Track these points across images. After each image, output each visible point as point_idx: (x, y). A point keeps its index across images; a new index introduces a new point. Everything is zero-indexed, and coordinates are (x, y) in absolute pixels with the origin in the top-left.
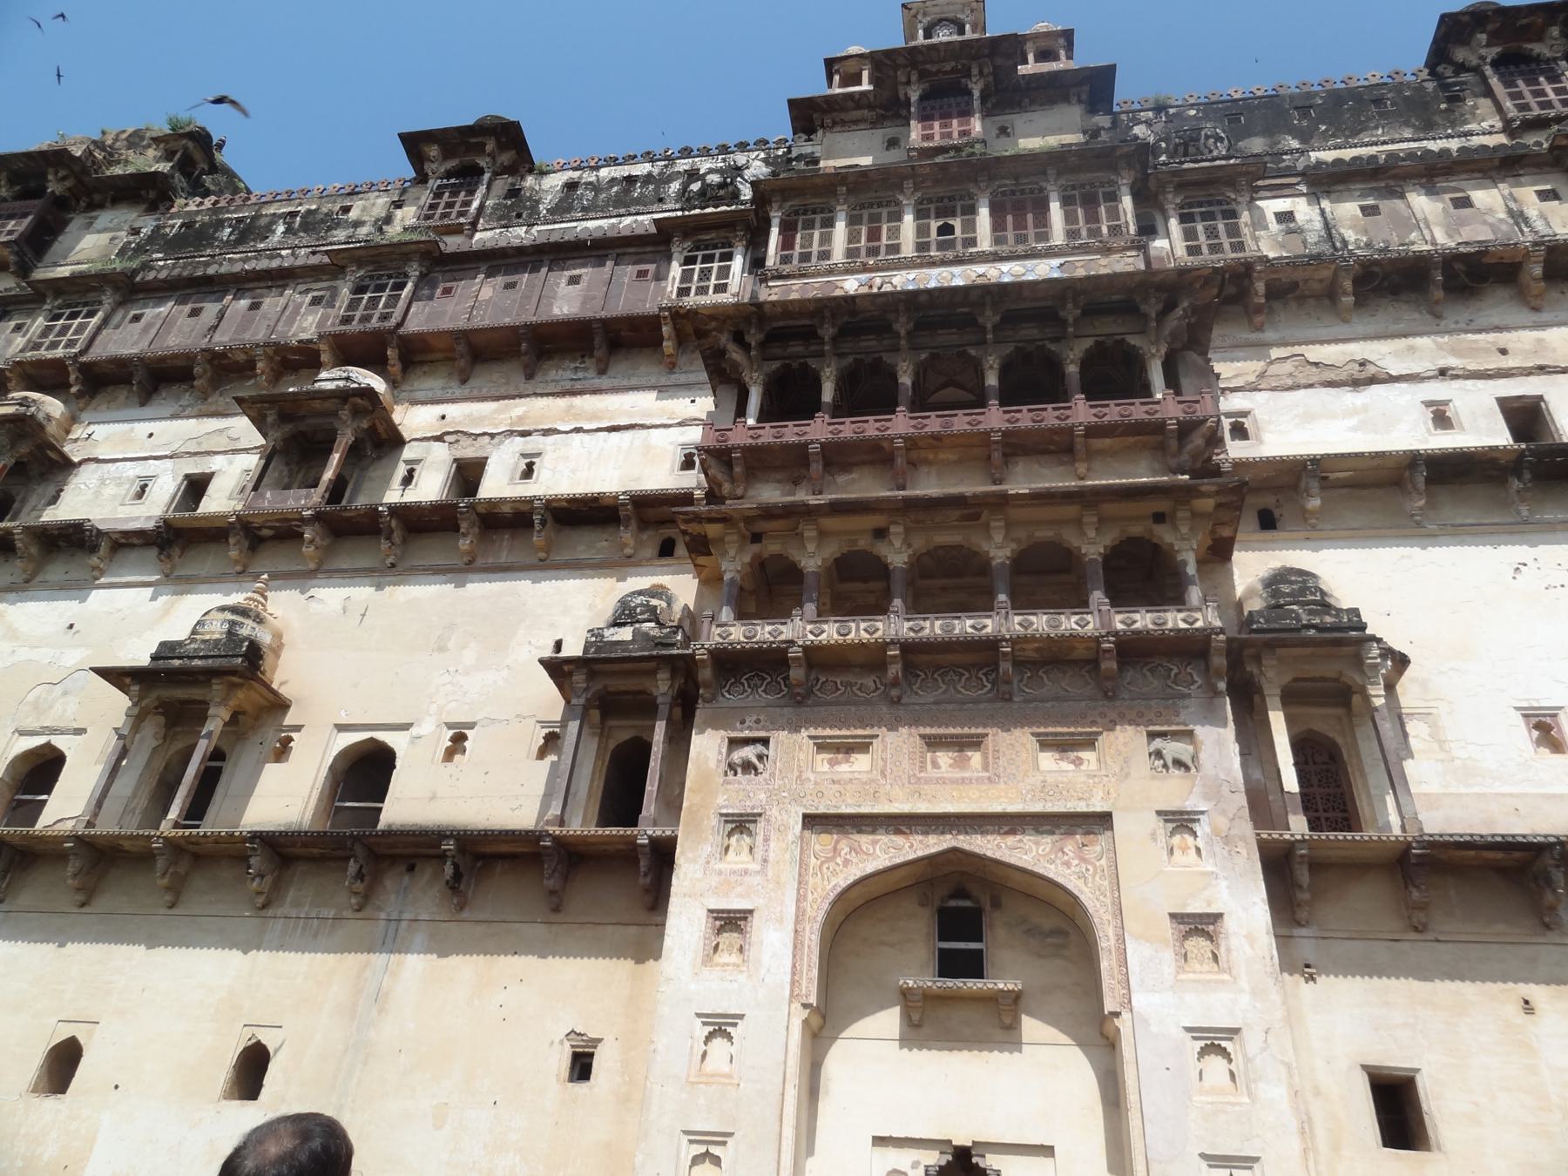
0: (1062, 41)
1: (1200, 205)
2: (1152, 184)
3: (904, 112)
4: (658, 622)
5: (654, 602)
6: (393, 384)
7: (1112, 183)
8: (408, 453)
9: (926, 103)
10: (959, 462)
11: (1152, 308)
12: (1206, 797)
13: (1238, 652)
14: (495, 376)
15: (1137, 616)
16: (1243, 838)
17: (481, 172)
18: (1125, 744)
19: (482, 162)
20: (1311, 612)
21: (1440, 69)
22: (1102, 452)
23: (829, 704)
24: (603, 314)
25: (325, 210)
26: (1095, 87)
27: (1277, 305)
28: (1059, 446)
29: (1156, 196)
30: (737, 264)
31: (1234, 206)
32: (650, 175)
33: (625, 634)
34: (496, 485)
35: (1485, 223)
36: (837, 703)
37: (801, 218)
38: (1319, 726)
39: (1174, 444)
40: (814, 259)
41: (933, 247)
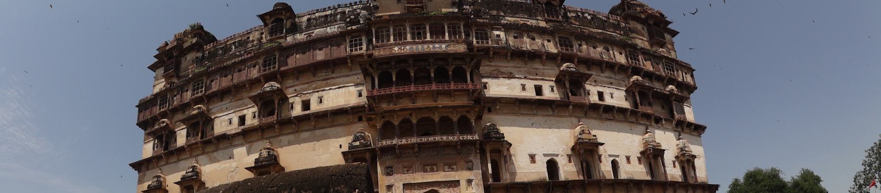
11: (468, 60)
28: (448, 94)
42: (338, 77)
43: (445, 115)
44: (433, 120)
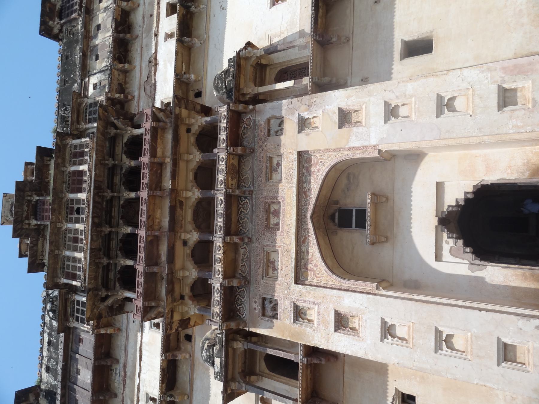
0: (29, 166)
1: (86, 116)
3: (42, 227)
4: (214, 345)
9: (38, 218)
11: (113, 131)
12: (293, 114)
15: (222, 138)
16: (309, 100)
18: (272, 145)
20: (229, 76)
21: (60, 38)
23: (250, 269)
27: (127, 91)
29: (81, 132)
31: (88, 104)
33: (217, 361)
35: (106, 20)
36: (250, 266)
38: (273, 77)
39: (161, 124)
42: (126, 356)
43: (191, 176)
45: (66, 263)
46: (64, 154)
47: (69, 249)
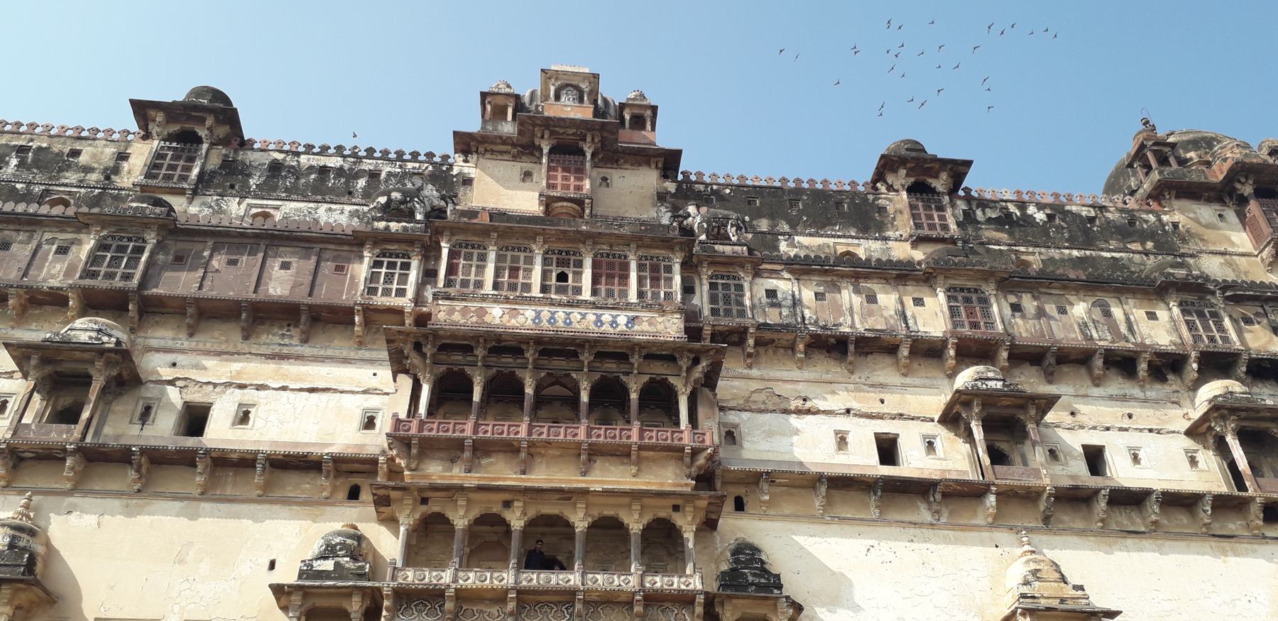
0: (649, 112)
1: (722, 277)
2: (695, 260)
5: (349, 541)
6: (132, 330)
7: (670, 259)
8: (150, 392)
10: (561, 456)
11: (684, 363)
13: (710, 601)
14: (216, 334)
15: (657, 579)
17: (199, 141)
19: (202, 133)
20: (754, 575)
21: (879, 185)
22: (647, 459)
24: (309, 301)
25: (56, 150)
26: (669, 161)
27: (761, 350)
28: (621, 454)
30: (413, 275)
32: (341, 168)
33: (328, 565)
34: (220, 432)
37: (464, 250)
39: (688, 460)
40: (471, 287)
41: (553, 290)
44: (569, 525)
45: (476, 252)
46: (657, 248)
47: (500, 258)
